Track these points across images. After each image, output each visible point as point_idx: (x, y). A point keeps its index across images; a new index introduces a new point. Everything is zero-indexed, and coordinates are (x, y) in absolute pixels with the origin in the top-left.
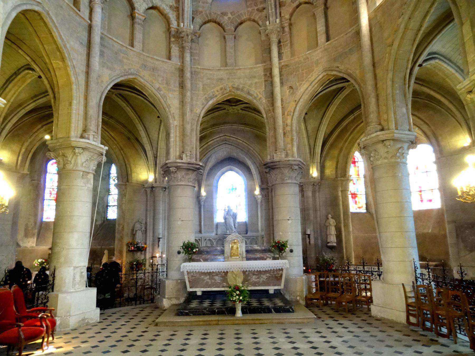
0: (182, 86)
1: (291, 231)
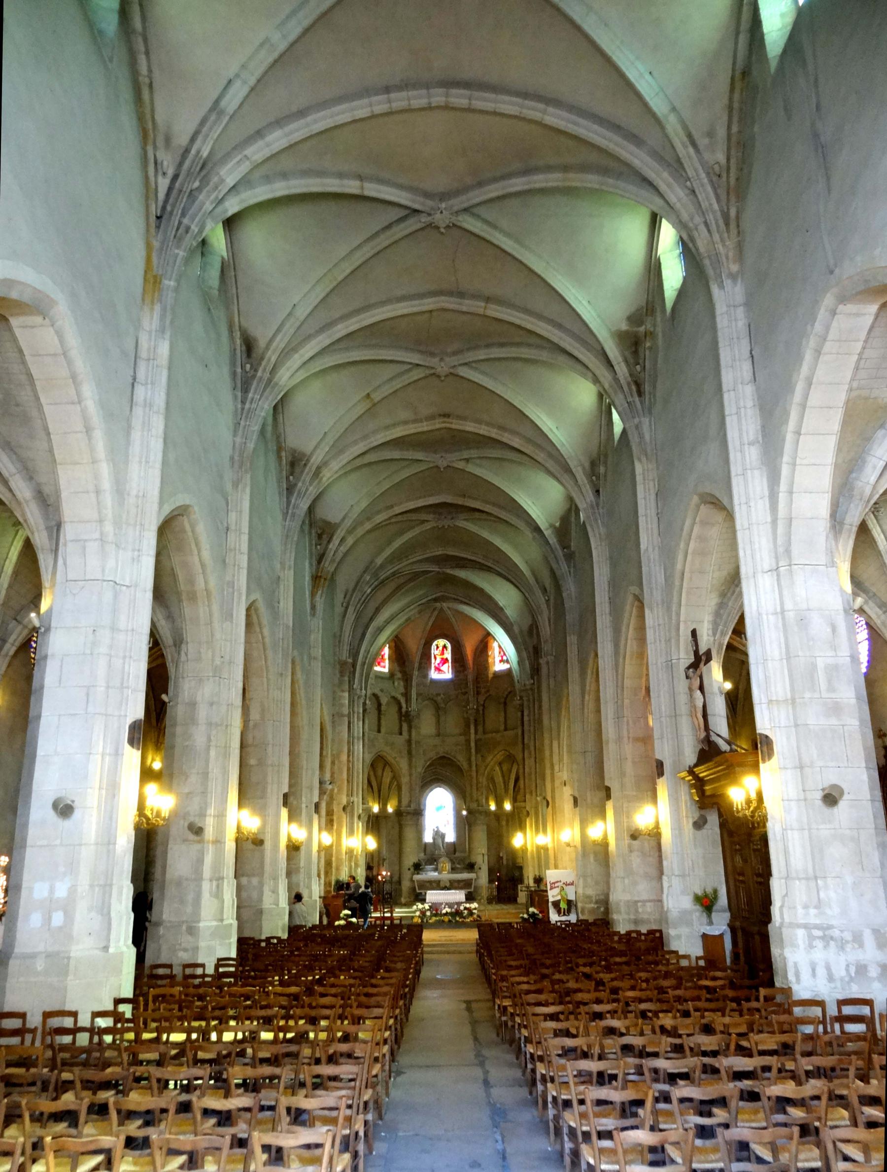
0: (410, 753)
1: (481, 855)
